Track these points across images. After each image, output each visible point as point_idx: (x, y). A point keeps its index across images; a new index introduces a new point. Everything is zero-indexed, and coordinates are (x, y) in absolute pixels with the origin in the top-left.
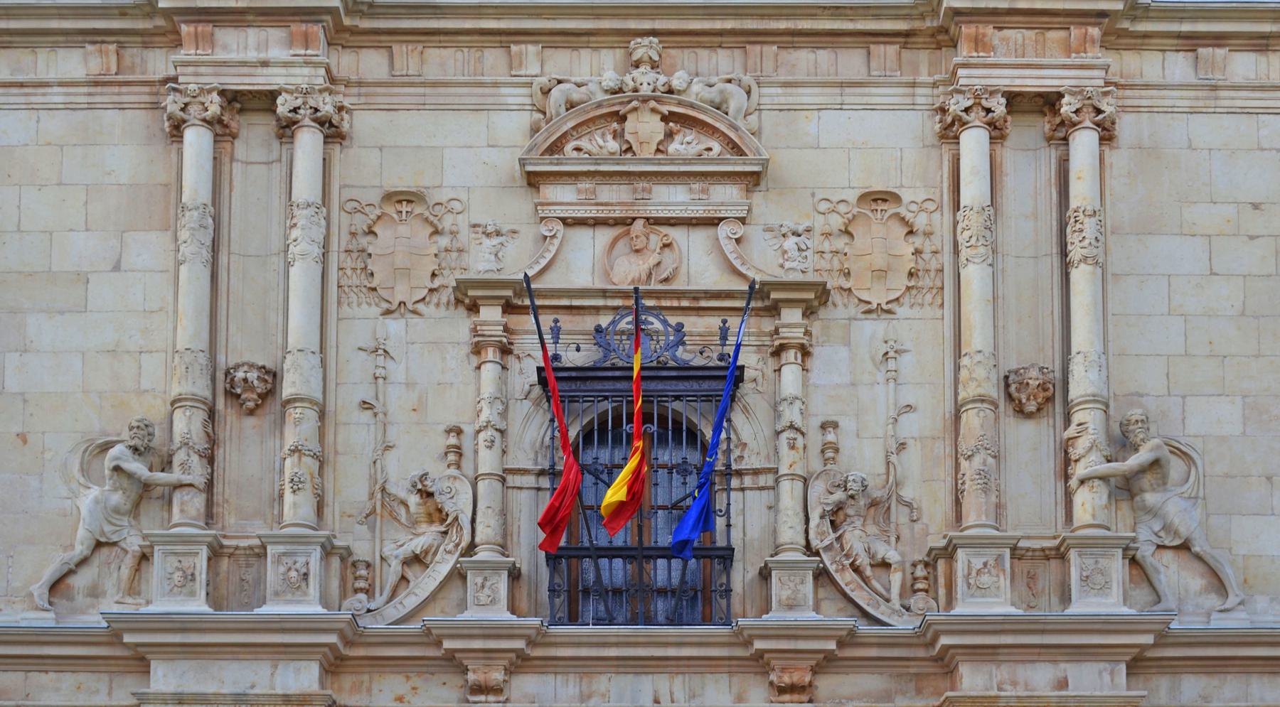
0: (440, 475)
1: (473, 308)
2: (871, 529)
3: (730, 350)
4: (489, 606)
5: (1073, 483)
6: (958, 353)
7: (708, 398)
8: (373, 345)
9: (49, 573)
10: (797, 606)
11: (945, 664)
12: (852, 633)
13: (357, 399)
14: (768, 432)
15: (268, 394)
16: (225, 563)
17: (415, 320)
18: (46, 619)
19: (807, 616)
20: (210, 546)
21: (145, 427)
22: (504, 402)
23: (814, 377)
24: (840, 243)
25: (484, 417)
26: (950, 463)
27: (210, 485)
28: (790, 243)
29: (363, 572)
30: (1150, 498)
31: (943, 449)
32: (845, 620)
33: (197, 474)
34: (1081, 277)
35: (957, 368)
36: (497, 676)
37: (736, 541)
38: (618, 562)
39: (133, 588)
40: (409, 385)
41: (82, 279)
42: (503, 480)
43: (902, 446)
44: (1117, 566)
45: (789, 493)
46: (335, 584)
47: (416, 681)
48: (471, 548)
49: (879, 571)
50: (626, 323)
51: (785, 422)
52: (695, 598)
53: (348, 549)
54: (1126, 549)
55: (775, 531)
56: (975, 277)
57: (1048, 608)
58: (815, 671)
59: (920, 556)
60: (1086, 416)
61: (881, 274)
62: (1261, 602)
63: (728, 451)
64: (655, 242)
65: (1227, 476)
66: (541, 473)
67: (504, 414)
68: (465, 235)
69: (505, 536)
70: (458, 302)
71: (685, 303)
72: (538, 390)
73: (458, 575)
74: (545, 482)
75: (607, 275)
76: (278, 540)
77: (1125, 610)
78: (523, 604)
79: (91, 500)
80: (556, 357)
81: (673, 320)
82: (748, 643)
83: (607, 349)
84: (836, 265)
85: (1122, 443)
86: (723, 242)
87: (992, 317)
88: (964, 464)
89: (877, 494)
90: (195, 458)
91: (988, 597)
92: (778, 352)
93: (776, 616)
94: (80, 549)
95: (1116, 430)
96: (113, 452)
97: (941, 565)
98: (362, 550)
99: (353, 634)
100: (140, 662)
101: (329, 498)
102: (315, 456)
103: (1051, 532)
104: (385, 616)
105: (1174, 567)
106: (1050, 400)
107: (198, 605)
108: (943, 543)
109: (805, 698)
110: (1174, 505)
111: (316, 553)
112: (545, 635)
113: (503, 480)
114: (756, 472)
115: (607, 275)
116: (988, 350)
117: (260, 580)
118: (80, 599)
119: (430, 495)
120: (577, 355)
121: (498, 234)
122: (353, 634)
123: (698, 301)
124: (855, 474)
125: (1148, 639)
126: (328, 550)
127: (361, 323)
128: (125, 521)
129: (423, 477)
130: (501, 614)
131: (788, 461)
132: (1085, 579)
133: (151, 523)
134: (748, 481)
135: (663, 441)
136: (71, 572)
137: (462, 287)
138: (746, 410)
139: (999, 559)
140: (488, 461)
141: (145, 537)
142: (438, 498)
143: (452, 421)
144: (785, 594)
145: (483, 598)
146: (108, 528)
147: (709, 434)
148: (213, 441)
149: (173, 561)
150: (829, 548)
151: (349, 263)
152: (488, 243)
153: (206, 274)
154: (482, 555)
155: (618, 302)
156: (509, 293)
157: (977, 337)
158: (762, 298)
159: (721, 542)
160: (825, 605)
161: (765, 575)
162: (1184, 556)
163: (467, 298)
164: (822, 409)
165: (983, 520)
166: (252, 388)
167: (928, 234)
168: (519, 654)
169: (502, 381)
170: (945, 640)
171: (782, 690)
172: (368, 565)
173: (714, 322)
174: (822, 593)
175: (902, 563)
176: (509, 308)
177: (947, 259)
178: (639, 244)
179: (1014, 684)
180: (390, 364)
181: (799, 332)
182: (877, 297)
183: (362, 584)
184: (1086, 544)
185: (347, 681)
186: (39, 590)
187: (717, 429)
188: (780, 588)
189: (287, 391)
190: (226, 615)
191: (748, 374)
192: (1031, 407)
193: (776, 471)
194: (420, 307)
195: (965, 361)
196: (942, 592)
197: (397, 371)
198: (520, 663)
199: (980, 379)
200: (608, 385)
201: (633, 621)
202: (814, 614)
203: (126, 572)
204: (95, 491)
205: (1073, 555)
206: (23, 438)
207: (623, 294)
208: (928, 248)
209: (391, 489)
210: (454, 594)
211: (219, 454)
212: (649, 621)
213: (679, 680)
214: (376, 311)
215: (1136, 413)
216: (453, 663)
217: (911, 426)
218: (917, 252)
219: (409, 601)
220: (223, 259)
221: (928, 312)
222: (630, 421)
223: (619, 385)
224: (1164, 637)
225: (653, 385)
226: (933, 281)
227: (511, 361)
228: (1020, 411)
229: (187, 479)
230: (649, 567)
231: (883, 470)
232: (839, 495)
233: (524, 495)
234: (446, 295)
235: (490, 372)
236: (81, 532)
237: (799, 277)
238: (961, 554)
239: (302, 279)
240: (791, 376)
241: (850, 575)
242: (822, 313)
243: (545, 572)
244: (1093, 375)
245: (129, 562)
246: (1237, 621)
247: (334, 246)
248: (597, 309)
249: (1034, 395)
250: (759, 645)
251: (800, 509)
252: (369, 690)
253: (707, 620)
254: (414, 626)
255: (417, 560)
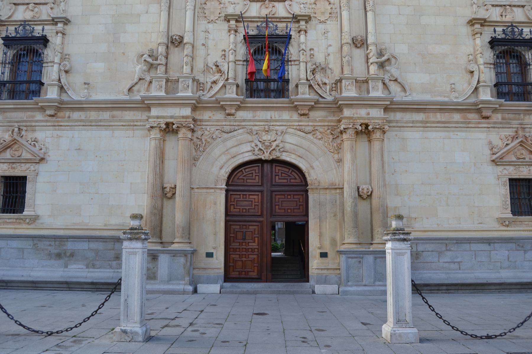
0: (220, 61)
1: (229, 21)
2: (322, 75)
3: (288, 31)
4: (231, 93)
5: (369, 64)
6: (341, 33)
7: (283, 43)
8: (205, 30)
9: (128, 87)
10: (304, 94)
11: (340, 109)
12: (318, 100)
13: (201, 43)
14: (297, 51)
15: (181, 42)
16: (169, 83)
17: (215, 24)
18: (127, 98)
19: (307, 96)
20: (166, 79)
21: (152, 50)
22: (235, 43)
23: (308, 38)
24: (314, 6)
25: (231, 47)
26: (340, 59)
27: (166, 64)
28: (302, 6)
29: (202, 85)
30: (388, 68)
31: (338, 55)
32: (317, 97)
33: (164, 61)
34: (370, 14)
35: (341, 36)
36: (233, 111)
37: (290, 78)
38: (262, 83)
39: (148, 90)
40: (213, 40)
41: (139, 15)
42: (235, 63)
43: (329, 55)
44: (380, 85)
45: (303, 66)
46: (195, 88)
47: (214, 113)
48: (228, 79)
49: (324, 85)
50: (264, 25)
51: (301, 48)
52: (280, 92)
53: (198, 80)
54: (382, 80)
55: (299, 75)
56: (345, 14)
57: (364, 95)
58: (309, 110)
59: (334, 82)
60: (372, 48)
61: (323, 13)
62: (414, 94)
63: (288, 56)
64: (271, 5)
65: (405, 63)
66: (244, 61)
67: (235, 47)
68: (227, 4)
69: (235, 76)
70: (225, 20)
71: (278, 20)
72: (243, 41)
73: (224, 86)
74: (245, 63)
75: (260, 13)
76: (182, 77)
77: (383, 95)
78: (240, 93)
79: (138, 69)
80: (248, 33)
81: (275, 24)
82: (293, 103)
83: (260, 31)
84: (313, 11)
85: (380, 54)
86: (287, 6)
87: (349, 24)
88: (344, 59)
89: (323, 66)
90: (163, 58)
91: (350, 92)
92: (299, 32)
93: (300, 96)
94: (136, 80)
95: (379, 51)
96: (144, 56)
97: (339, 84)
98: (202, 80)
99: (199, 101)
100: (148, 108)
101: (194, 67)
102: (191, 57)
103: (364, 76)
104: (207, 96)
105: (393, 85)
106: (363, 44)
107: (163, 94)
108: (339, 78)
109: (307, 117)
110: (393, 70)
111: (191, 81)
112: (245, 101)
113: (235, 63)
114: (295, 61)
115: (260, 13)
116: (349, 31)
117: (177, 88)
118: (135, 93)
119: (218, 66)
120: (253, 32)
121: (235, 4)
122: (199, 101)
123: (281, 19)
124: (318, 61)
125: (388, 103)
126: (194, 80)
127: (203, 25)
128: (146, 73)
129: (216, 62)
130: (234, 96)
131: (302, 58)
132: (373, 88)
133: (153, 74)
134: (293, 63)
135: (273, 54)
136: (133, 86)
137: (226, 16)
138: (292, 46)
139: (352, 82)
140: (232, 58)
141: (151, 77)
142: (220, 67)
143: (223, 48)
144: (302, 91)
145: (230, 92)
146: (142, 75)
147: (283, 51)
148: (167, 53)
149: (157, 82)
150: (312, 79)
151: (200, 11)
152: (232, 6)
153: (167, 13)
154: (230, 81)
155: (262, 20)
156: (237, 17)
157: (346, 28)
158: (296, 19)
159: (286, 78)
160: (311, 94)
161: (297, 86)
162: (396, 82)
163: (227, 19)
164: (310, 46)
165: (348, 73)
166: (177, 41)
167: (334, 4)
168: (239, 106)
169: (235, 39)
170: (340, 102)
171: (301, 115)
172: (203, 84)
173: (284, 25)
174: (310, 91)
175: (329, 83)
176: (237, 21)
177: (338, 10)
178: (267, 6)
179: (357, 114)
180: (209, 35)
181: (304, 27)
182: (322, 19)
183: (201, 88)
184: (373, 79)
185: (198, 113)
186: (126, 90)
187: (286, 50)
188: (300, 89)
189: (185, 41)
190: (169, 96)
191: (293, 37)
192: (359, 45)
193: (299, 60)
194: (216, 21)
195: (343, 34)
196: (339, 91)
197: (211, 36)
198: (239, 108)
199: (347, 39)
200: (260, 39)
201: (266, 97)
202: (308, 96)
203: (146, 86)
204: (140, 66)
205: (370, 81)
206: (124, 53)
207: (264, 18)
208: (334, 7)
209: (209, 65)
210: (223, 91)
211: (169, 57)
212: (269, 97)
213: (276, 112)
214: (206, 22)
215: (383, 47)
216: (223, 108)
217: (331, 50)
218: (331, 8)
219: (213, 93)
220: (171, 10)
221: (334, 22)
222: (265, 48)
223: (263, 39)
224: (392, 103)
225: (270, 39)
226: (335, 15)
227: (237, 34)
228: (356, 46)
229: (161, 63)
230: (269, 84)
231: (324, 60)
232: (314, 66)
233: (240, 66)
234: (223, 18)
235: (232, 36)
236: (136, 76)
237: (304, 14)
238: (343, 81)
239: (189, 14)
240: (302, 37)
241: (317, 86)
242: (310, 22)
243: (245, 85)
244: (373, 38)
245: (147, 83)
246: (409, 99)
247: (197, 7)
248: (257, 21)
249: (359, 43)
250: (296, 103)
251: (305, 70)
252: (203, 115)
253: (283, 97)
254: (214, 99)
255: (215, 82)
